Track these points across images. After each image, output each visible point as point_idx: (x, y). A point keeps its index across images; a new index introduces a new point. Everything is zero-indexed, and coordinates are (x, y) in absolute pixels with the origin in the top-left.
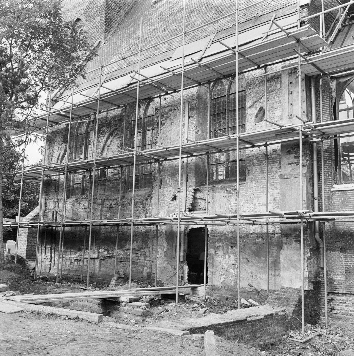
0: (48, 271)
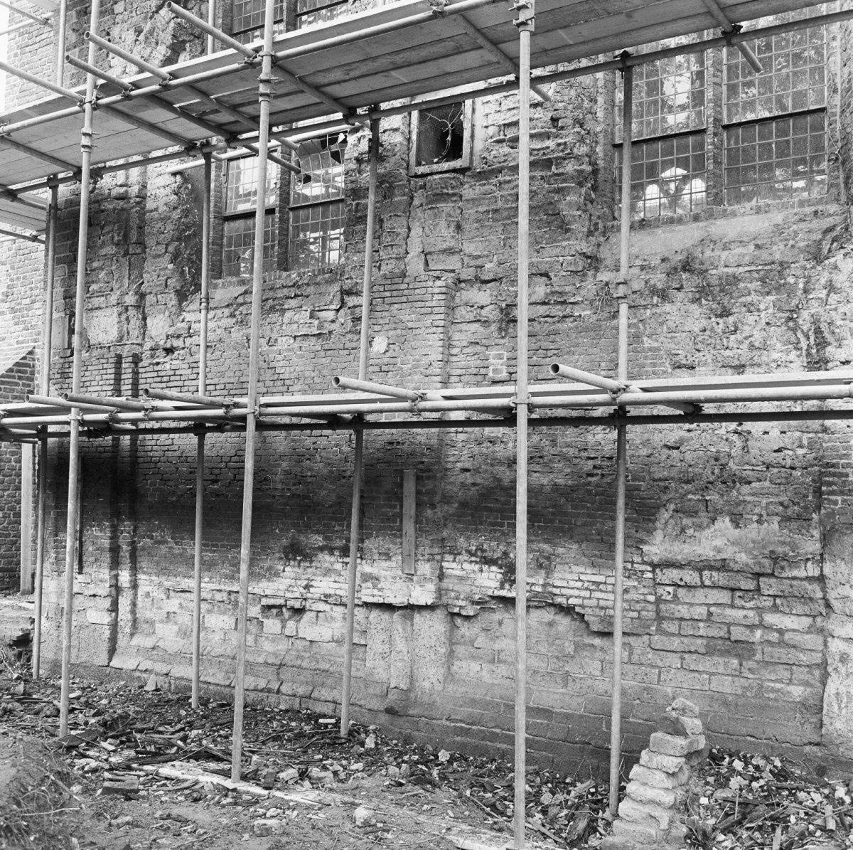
0: (102, 659)
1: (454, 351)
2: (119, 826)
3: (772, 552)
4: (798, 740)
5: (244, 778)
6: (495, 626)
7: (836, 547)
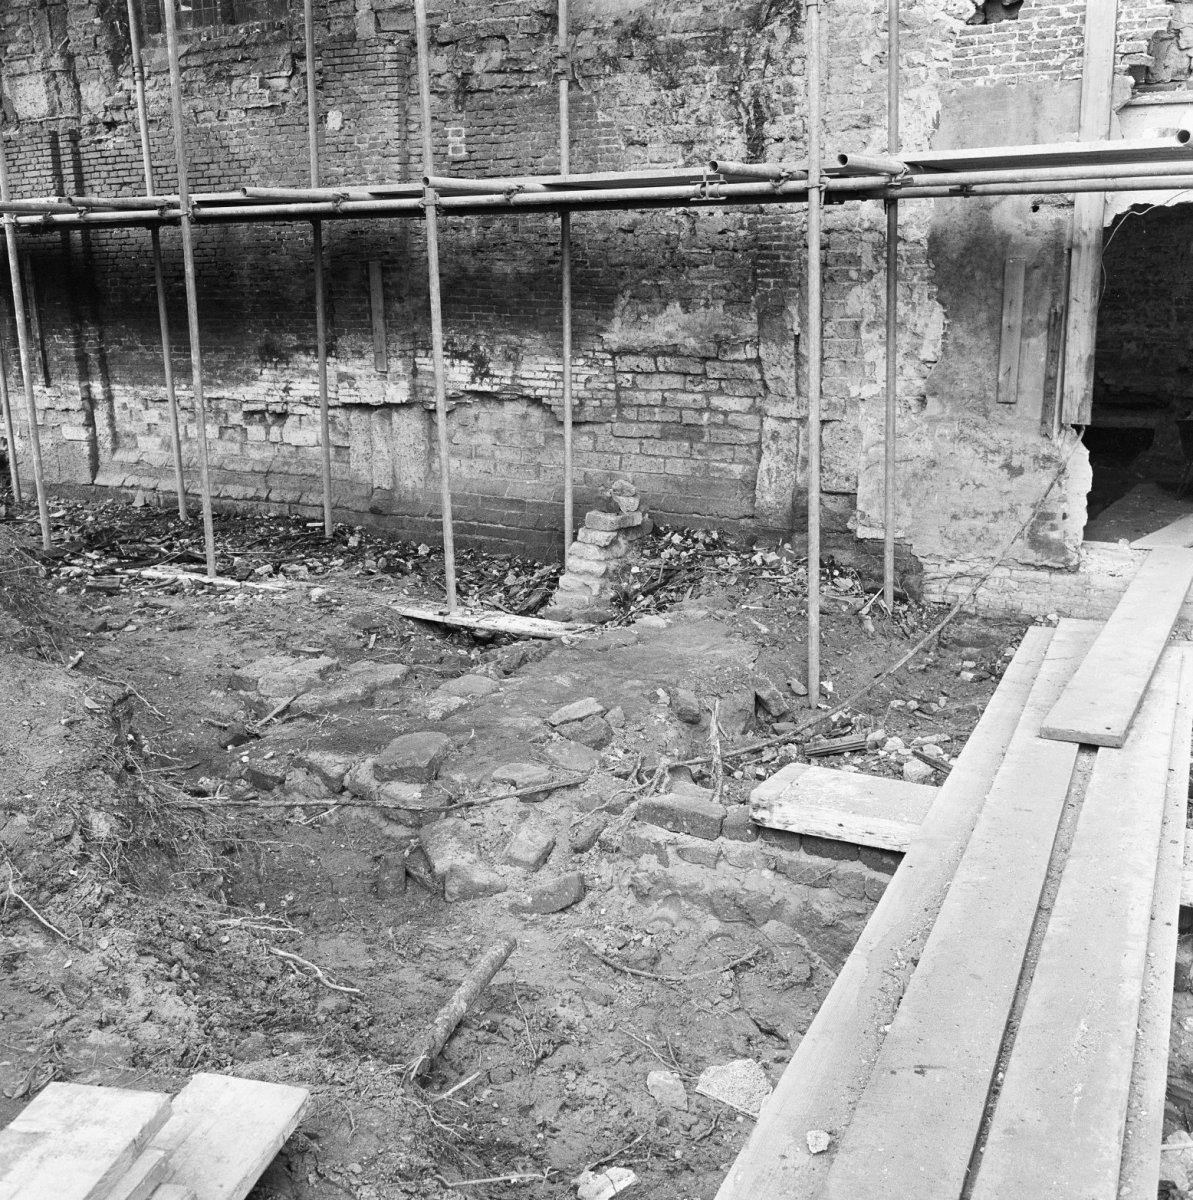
0: (85, 477)
1: (413, 127)
2: (100, 614)
3: (716, 336)
4: (735, 514)
5: (220, 574)
6: (472, 421)
7: (767, 330)
